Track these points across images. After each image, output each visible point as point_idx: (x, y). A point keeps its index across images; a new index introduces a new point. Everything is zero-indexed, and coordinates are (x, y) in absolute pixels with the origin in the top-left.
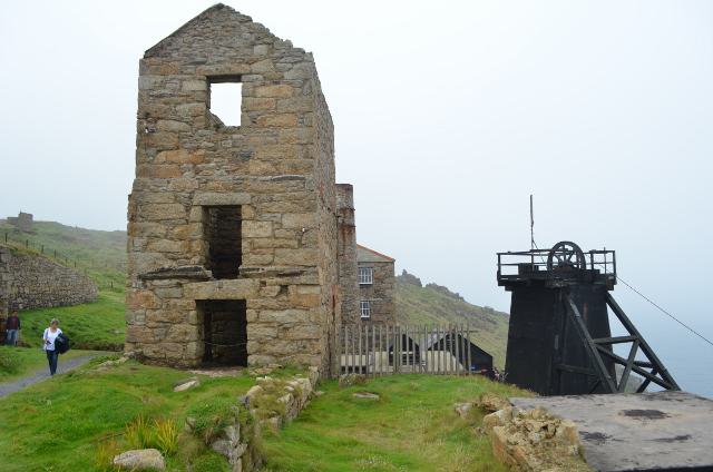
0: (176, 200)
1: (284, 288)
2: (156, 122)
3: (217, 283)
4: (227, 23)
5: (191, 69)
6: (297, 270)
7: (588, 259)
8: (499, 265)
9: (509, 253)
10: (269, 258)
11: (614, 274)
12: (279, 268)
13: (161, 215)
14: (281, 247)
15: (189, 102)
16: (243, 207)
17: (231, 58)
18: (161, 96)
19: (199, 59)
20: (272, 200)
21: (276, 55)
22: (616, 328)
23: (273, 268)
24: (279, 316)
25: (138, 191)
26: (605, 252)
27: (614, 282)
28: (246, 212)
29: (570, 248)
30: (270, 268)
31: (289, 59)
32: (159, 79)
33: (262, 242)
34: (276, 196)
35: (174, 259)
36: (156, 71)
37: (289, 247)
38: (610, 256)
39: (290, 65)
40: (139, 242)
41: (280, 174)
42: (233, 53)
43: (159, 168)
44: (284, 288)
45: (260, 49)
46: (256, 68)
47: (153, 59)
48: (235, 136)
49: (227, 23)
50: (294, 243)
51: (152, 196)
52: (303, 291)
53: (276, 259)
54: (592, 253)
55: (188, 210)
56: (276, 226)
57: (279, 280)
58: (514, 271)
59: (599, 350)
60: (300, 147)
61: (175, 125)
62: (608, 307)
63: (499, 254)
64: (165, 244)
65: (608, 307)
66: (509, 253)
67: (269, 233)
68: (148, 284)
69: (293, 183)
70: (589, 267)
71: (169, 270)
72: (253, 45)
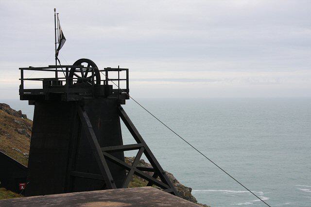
7: (103, 76)
8: (22, 79)
9: (31, 68)
11: (127, 90)
22: (127, 139)
26: (119, 70)
27: (127, 97)
29: (85, 65)
38: (123, 74)
54: (107, 70)
58: (39, 85)
59: (105, 157)
63: (22, 70)
66: (31, 68)
70: (102, 83)
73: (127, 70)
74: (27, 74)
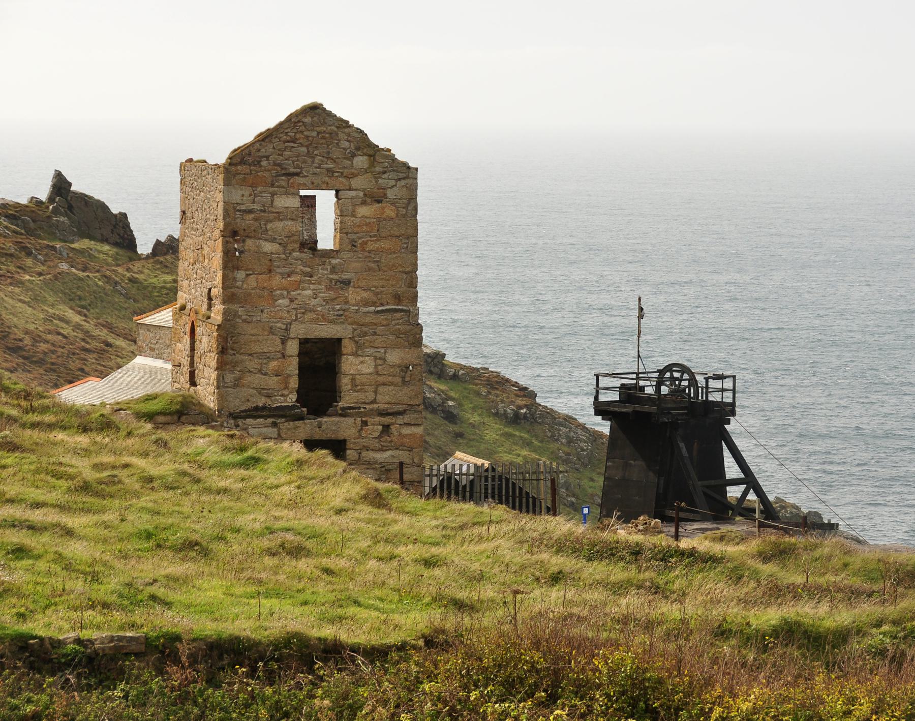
0: (272, 331)
1: (386, 428)
2: (244, 241)
3: (315, 422)
4: (323, 128)
5: (283, 181)
6: (400, 408)
10: (371, 396)
11: (733, 404)
12: (382, 406)
13: (257, 348)
14: (384, 384)
15: (282, 220)
16: (345, 342)
17: (328, 170)
18: (251, 211)
19: (292, 170)
20: (375, 334)
21: (378, 169)
22: (732, 470)
23: (375, 406)
24: (380, 456)
25: (229, 320)
26: (722, 377)
27: (733, 413)
28: (348, 346)
30: (371, 406)
31: (392, 175)
32: (247, 191)
33: (364, 379)
34: (380, 329)
35: (269, 396)
36: (243, 182)
37: (392, 384)
38: (728, 384)
39: (393, 183)
40: (229, 378)
41: (382, 305)
42: (330, 165)
43: (250, 294)
44: (386, 428)
45: (361, 161)
46: (355, 183)
47: (239, 168)
48: (334, 261)
49: (323, 128)
50: (398, 380)
51: (245, 325)
52: (406, 431)
53: (379, 397)
55: (283, 342)
56: (379, 362)
57: (377, 419)
58: (614, 396)
59: (705, 494)
60: (405, 276)
61: (268, 247)
62: (723, 443)
63: (597, 376)
64: (255, 380)
65: (723, 443)
67: (371, 369)
68: (240, 422)
69: (398, 315)
71: (264, 408)
72: (354, 155)
73: (734, 377)
74: (604, 381)
